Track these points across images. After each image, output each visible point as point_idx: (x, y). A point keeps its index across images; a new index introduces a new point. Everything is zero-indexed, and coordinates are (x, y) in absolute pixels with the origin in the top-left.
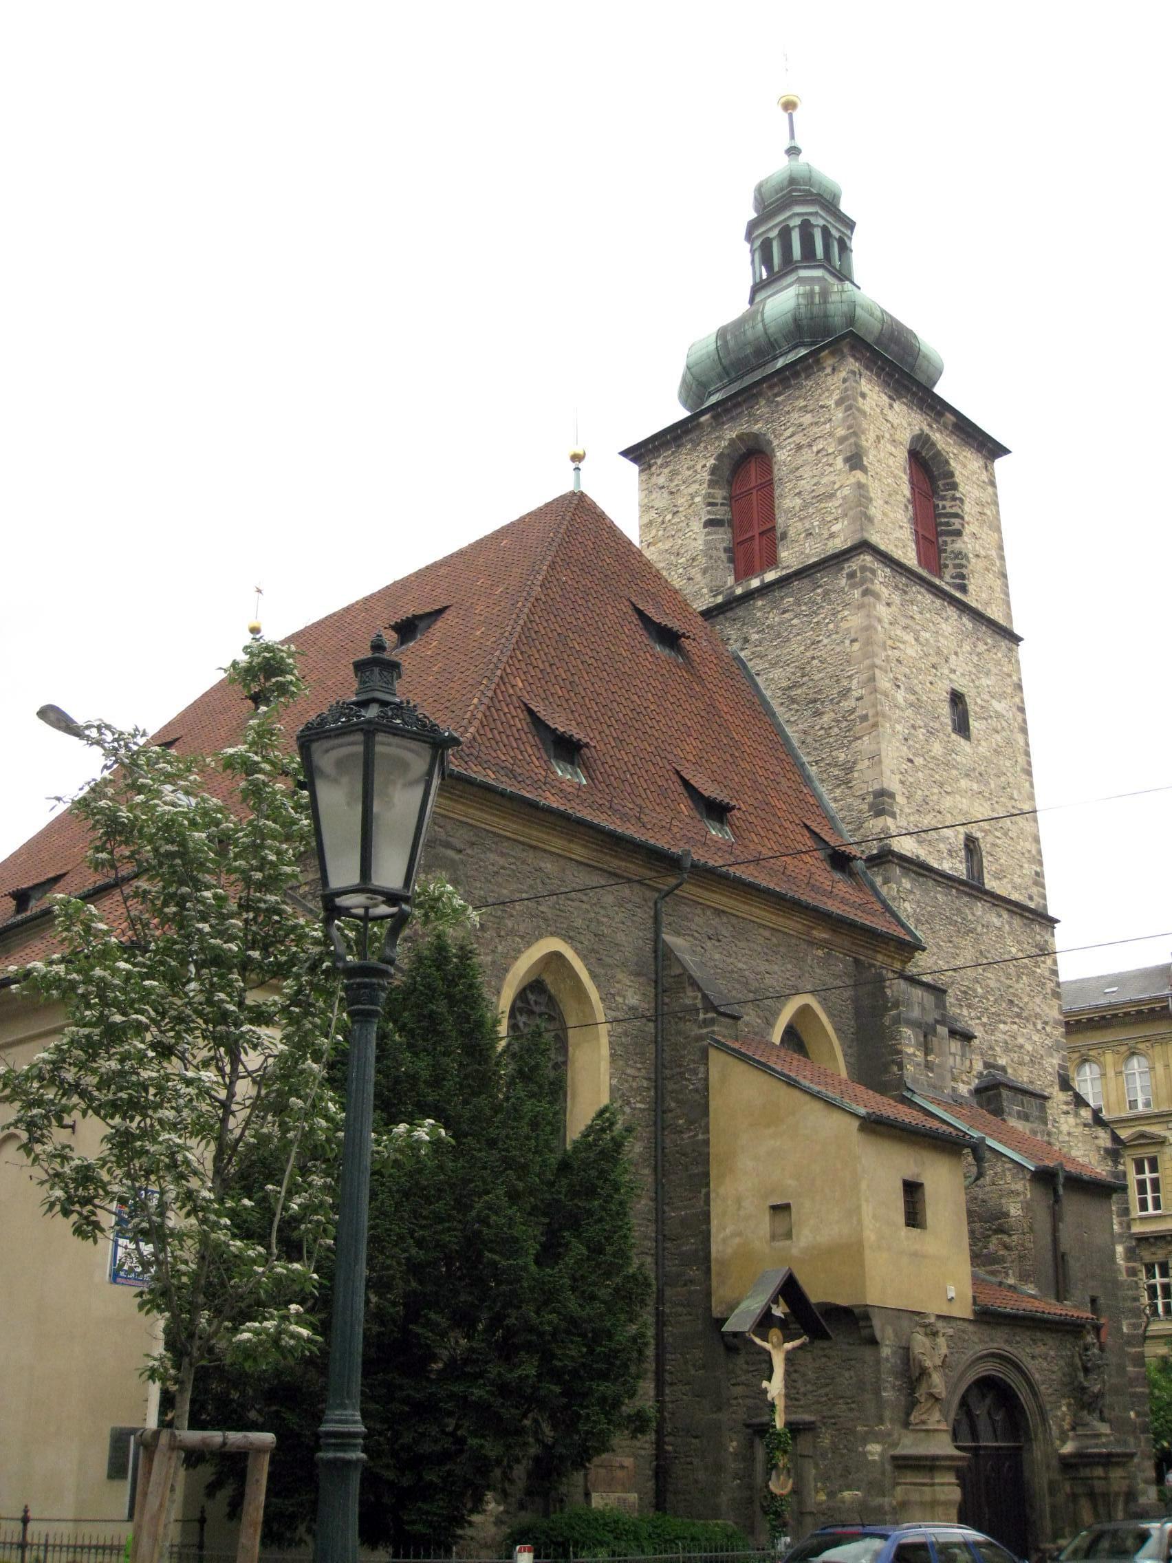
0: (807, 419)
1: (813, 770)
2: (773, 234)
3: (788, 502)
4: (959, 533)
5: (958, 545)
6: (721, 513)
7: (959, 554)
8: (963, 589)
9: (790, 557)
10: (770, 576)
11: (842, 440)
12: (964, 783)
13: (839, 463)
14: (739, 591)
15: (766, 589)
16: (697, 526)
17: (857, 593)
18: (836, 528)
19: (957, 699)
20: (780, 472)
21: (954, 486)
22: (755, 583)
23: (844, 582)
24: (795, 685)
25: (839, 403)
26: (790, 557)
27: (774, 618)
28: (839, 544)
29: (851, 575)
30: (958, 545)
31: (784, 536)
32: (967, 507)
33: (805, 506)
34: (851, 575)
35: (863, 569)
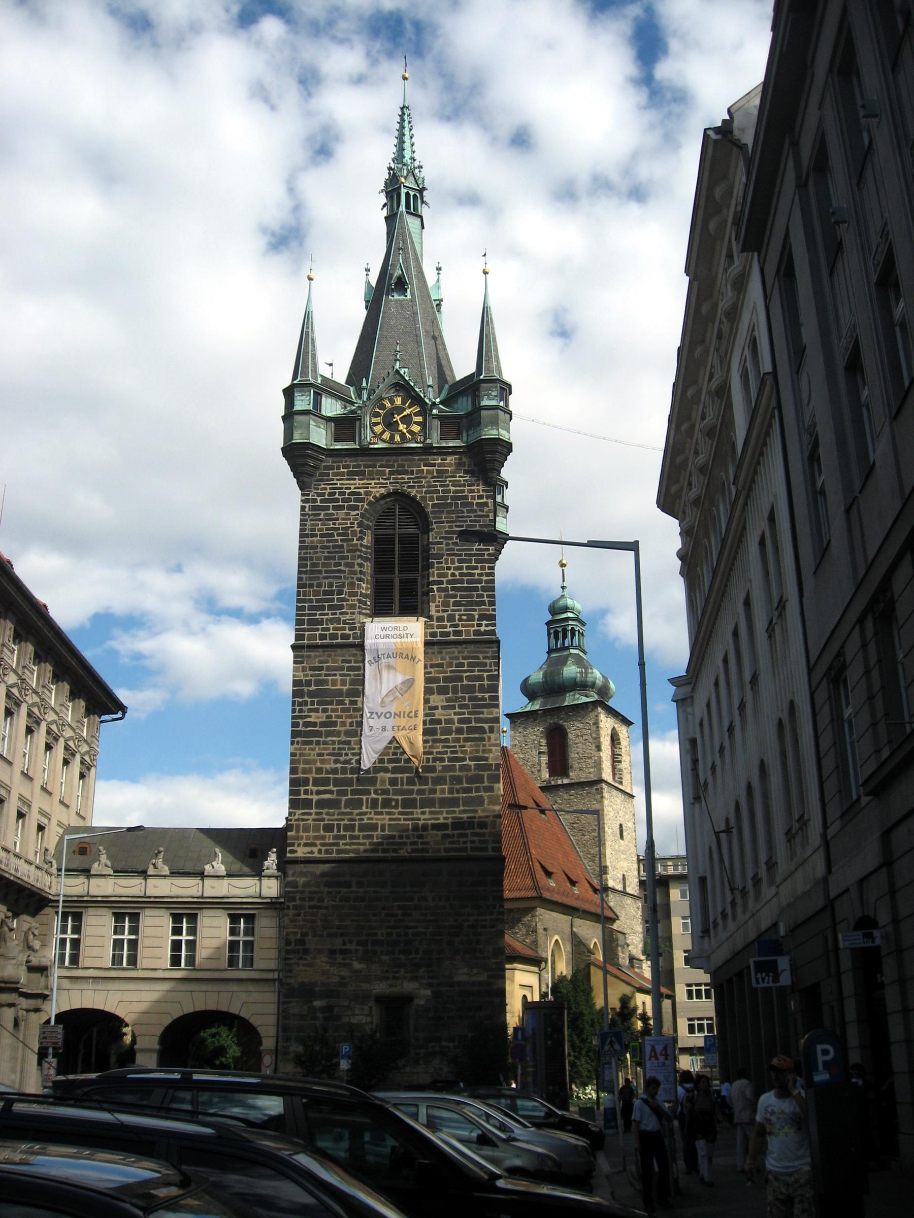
0: (581, 726)
1: (581, 854)
2: (560, 630)
3: (573, 755)
4: (620, 762)
5: (620, 767)
6: (544, 749)
7: (620, 770)
8: (621, 783)
9: (575, 775)
10: (566, 781)
11: (595, 739)
12: (623, 856)
13: (593, 747)
14: (553, 783)
15: (563, 786)
16: (535, 753)
17: (599, 796)
18: (592, 770)
19: (621, 825)
20: (571, 742)
21: (620, 744)
22: (560, 782)
23: (594, 791)
24: (575, 823)
25: (594, 724)
26: (575, 775)
27: (566, 796)
28: (593, 778)
29: (597, 790)
30: (620, 767)
31: (571, 767)
32: (623, 750)
33: (580, 758)
34: (597, 790)
35: (602, 788)
